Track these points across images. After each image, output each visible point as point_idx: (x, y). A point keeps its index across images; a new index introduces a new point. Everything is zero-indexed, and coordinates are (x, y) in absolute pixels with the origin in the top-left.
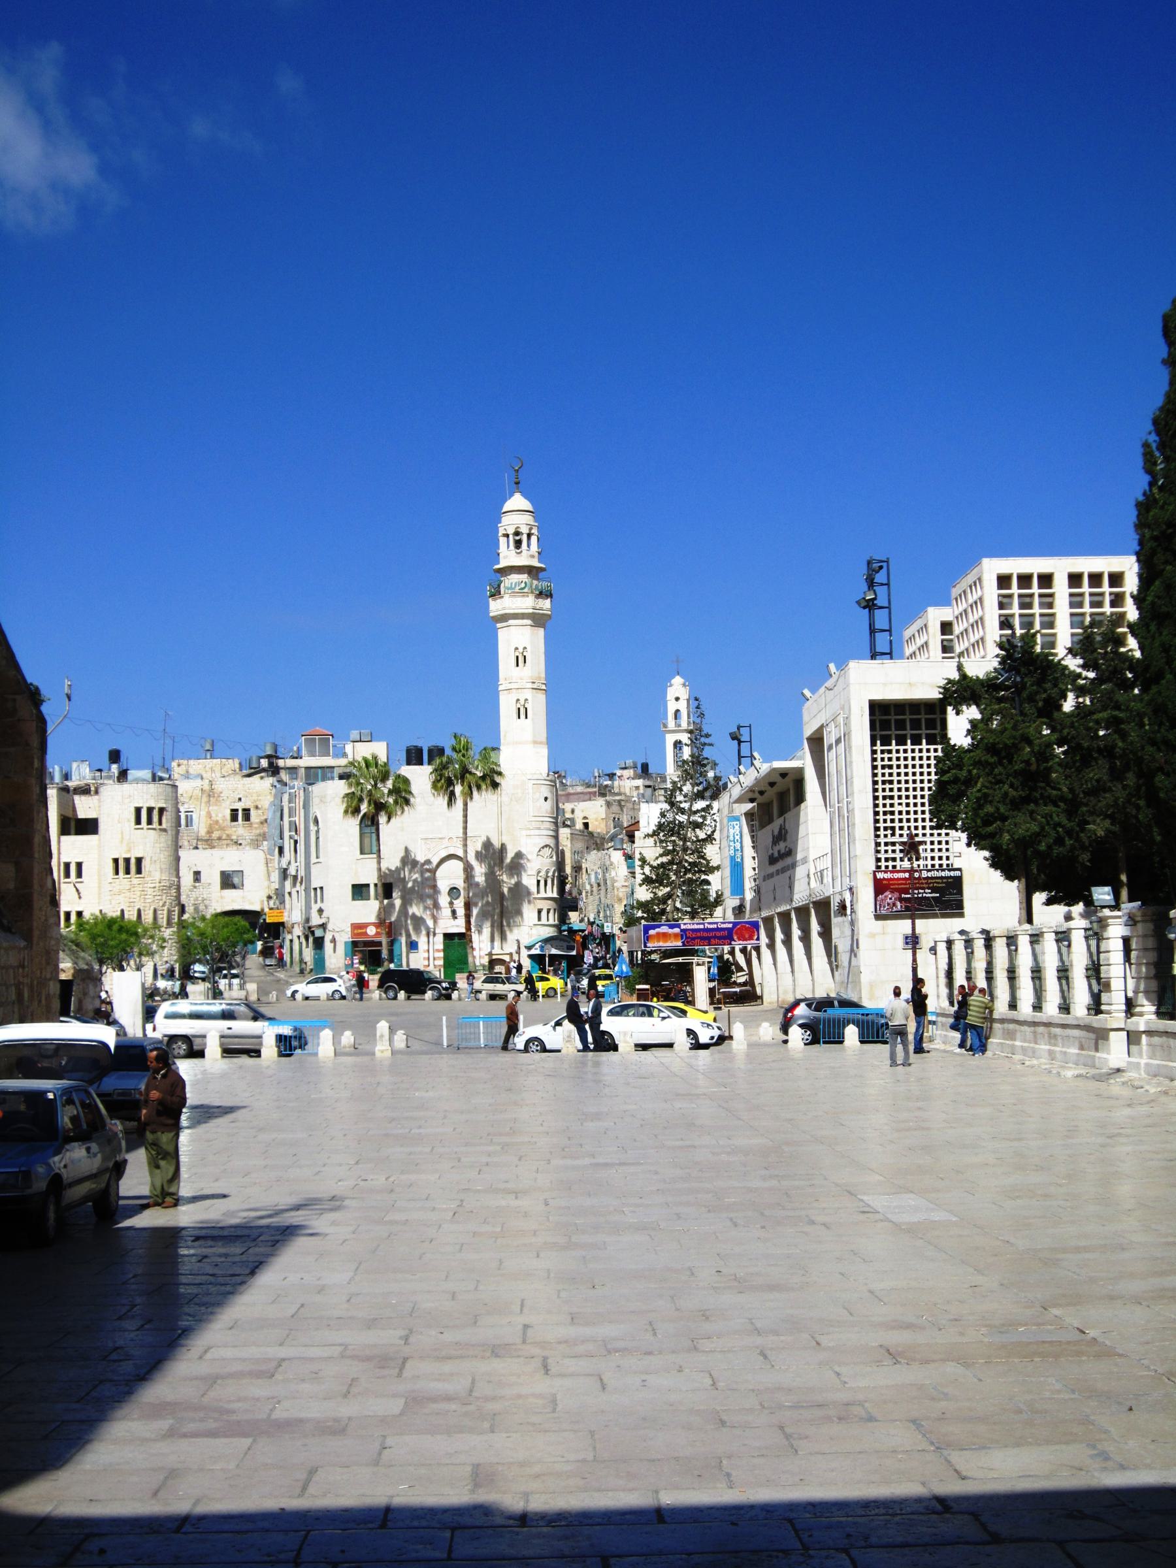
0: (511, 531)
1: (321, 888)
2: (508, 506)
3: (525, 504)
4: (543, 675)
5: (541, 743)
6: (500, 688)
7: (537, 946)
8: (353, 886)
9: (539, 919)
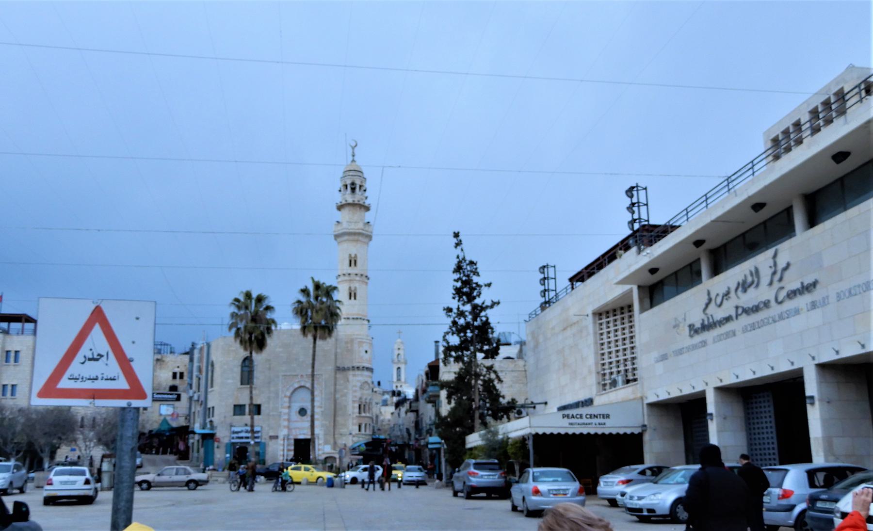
8: (235, 406)
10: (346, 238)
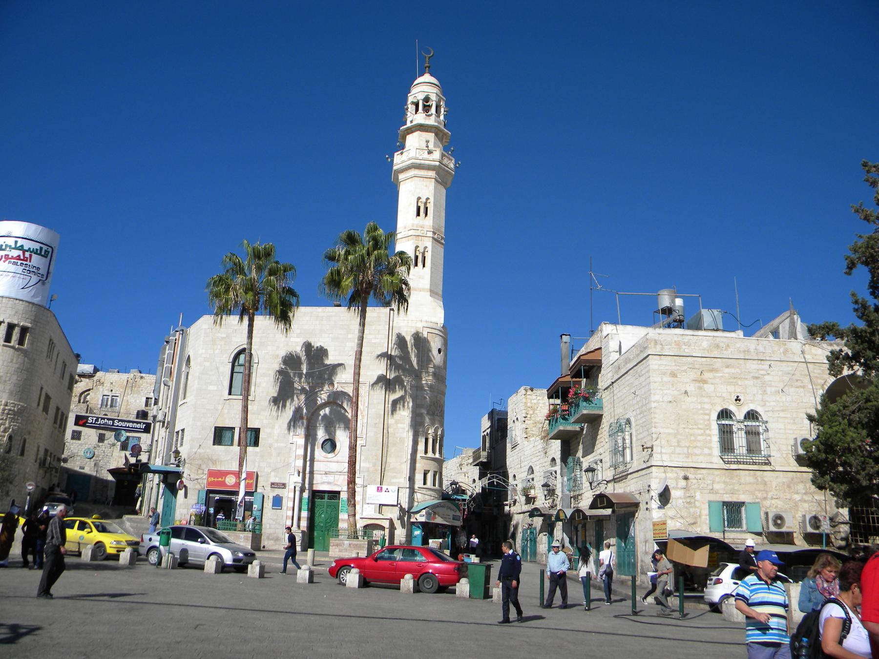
0: (421, 97)
1: (183, 430)
2: (420, 80)
3: (433, 80)
4: (443, 230)
5: (437, 294)
6: (399, 236)
7: (424, 512)
9: (425, 483)
10: (413, 172)
